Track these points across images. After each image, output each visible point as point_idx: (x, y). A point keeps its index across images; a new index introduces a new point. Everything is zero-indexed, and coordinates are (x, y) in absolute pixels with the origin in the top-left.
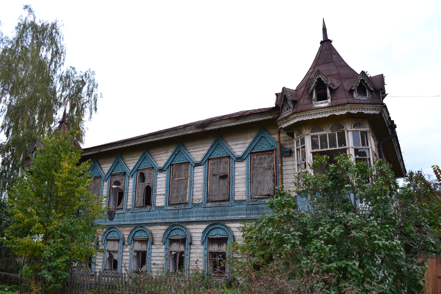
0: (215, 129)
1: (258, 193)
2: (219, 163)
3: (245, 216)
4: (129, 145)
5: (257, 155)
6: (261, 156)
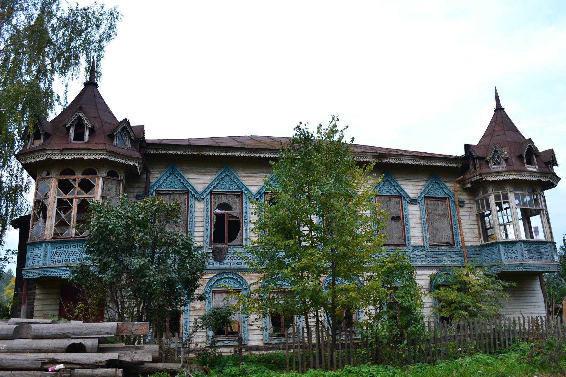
0: (395, 164)
3: (424, 263)
4: (262, 155)
5: (430, 200)
6: (435, 202)
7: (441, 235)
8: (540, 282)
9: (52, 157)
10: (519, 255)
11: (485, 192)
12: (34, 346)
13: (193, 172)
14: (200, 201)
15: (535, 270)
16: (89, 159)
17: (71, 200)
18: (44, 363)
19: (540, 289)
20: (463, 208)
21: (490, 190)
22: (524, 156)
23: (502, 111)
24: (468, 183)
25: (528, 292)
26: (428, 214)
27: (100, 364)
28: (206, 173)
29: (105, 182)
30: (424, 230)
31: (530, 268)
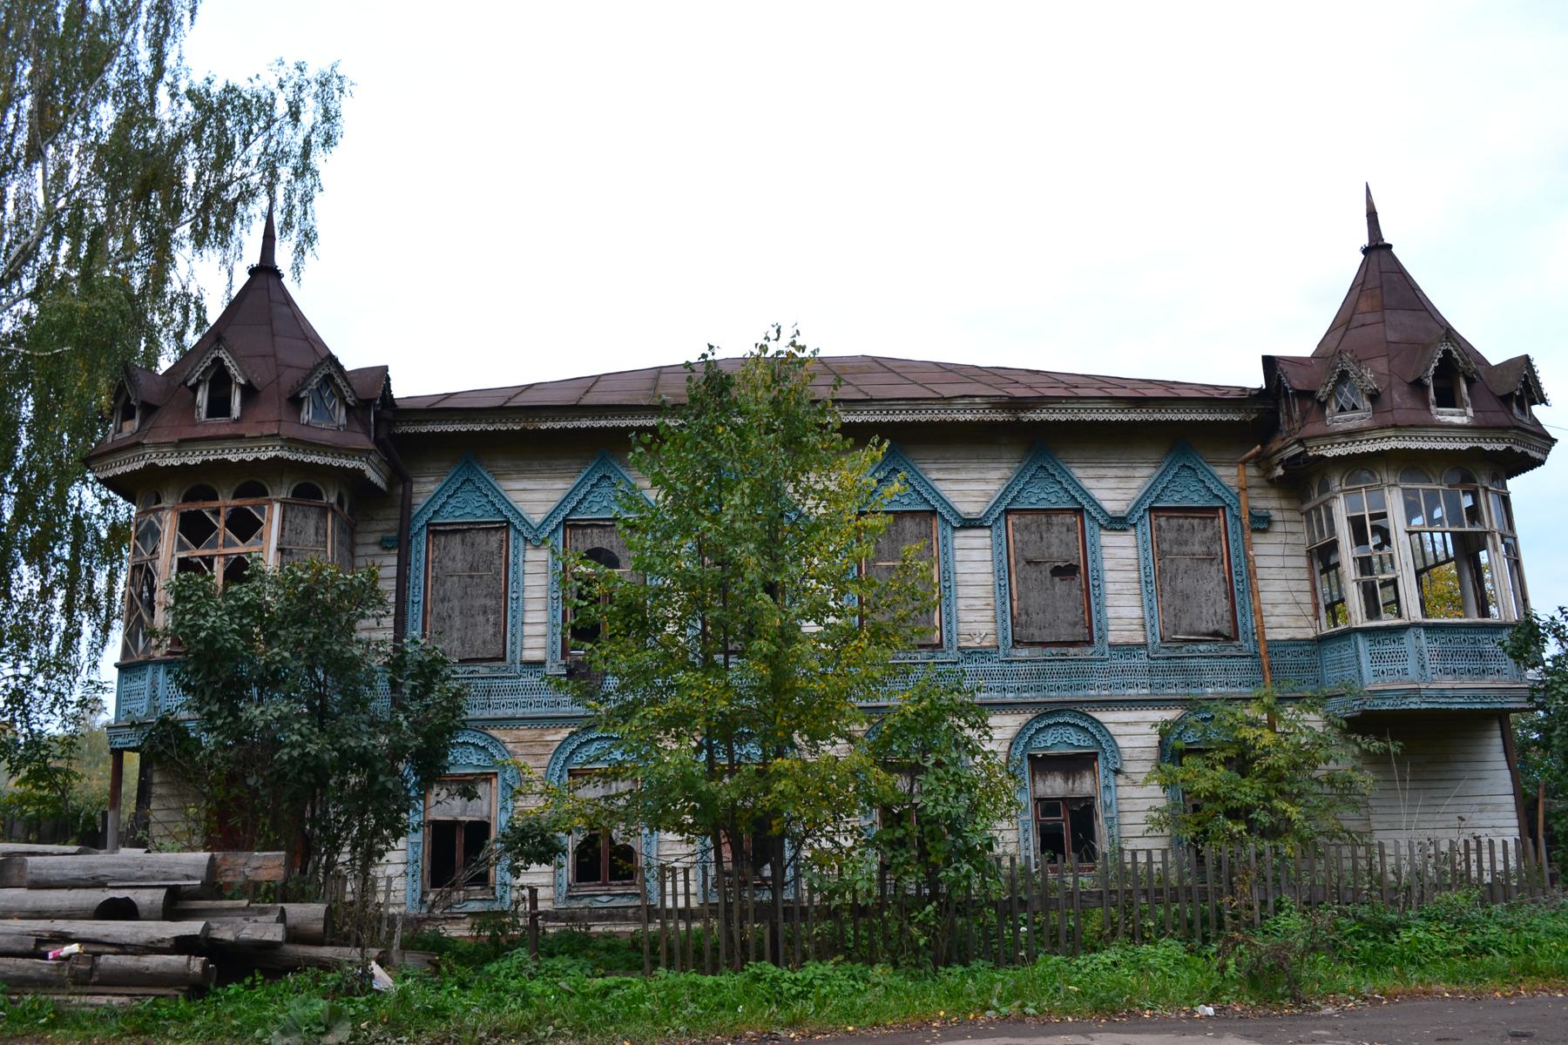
0: (1057, 423)
1: (1185, 624)
2: (1044, 527)
3: (1145, 691)
5: (1168, 518)
6: (1181, 521)
7: (1196, 611)
8: (1503, 737)
9: (157, 461)
10: (1412, 666)
11: (1325, 488)
12: (29, 905)
13: (521, 472)
14: (537, 547)
15: (1457, 706)
16: (242, 461)
17: (209, 561)
18: (40, 941)
19: (1502, 757)
20: (1268, 535)
21: (1335, 483)
22: (1429, 382)
23: (1384, 253)
24: (1277, 465)
25: (1461, 766)
26: (1161, 555)
27: (160, 945)
28: (552, 472)
29: (289, 515)
30: (1145, 601)
31: (1441, 700)
